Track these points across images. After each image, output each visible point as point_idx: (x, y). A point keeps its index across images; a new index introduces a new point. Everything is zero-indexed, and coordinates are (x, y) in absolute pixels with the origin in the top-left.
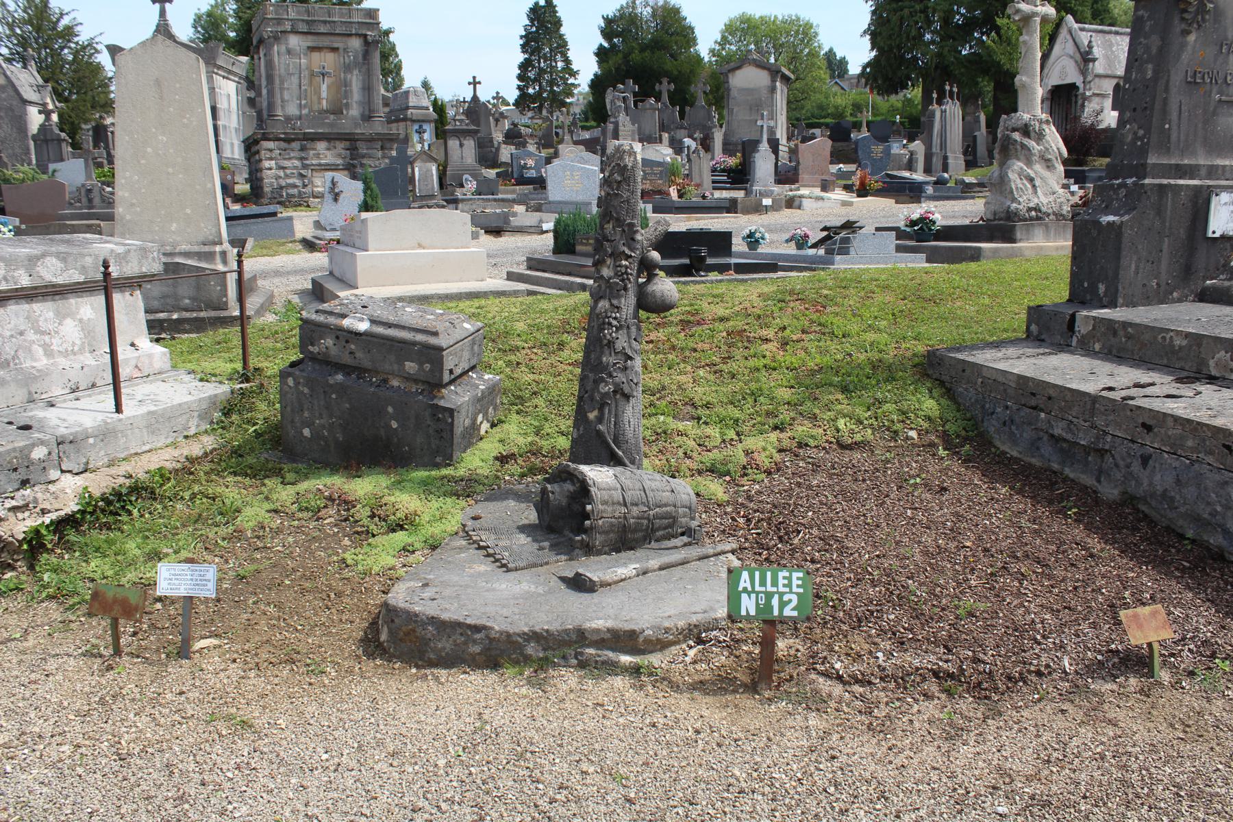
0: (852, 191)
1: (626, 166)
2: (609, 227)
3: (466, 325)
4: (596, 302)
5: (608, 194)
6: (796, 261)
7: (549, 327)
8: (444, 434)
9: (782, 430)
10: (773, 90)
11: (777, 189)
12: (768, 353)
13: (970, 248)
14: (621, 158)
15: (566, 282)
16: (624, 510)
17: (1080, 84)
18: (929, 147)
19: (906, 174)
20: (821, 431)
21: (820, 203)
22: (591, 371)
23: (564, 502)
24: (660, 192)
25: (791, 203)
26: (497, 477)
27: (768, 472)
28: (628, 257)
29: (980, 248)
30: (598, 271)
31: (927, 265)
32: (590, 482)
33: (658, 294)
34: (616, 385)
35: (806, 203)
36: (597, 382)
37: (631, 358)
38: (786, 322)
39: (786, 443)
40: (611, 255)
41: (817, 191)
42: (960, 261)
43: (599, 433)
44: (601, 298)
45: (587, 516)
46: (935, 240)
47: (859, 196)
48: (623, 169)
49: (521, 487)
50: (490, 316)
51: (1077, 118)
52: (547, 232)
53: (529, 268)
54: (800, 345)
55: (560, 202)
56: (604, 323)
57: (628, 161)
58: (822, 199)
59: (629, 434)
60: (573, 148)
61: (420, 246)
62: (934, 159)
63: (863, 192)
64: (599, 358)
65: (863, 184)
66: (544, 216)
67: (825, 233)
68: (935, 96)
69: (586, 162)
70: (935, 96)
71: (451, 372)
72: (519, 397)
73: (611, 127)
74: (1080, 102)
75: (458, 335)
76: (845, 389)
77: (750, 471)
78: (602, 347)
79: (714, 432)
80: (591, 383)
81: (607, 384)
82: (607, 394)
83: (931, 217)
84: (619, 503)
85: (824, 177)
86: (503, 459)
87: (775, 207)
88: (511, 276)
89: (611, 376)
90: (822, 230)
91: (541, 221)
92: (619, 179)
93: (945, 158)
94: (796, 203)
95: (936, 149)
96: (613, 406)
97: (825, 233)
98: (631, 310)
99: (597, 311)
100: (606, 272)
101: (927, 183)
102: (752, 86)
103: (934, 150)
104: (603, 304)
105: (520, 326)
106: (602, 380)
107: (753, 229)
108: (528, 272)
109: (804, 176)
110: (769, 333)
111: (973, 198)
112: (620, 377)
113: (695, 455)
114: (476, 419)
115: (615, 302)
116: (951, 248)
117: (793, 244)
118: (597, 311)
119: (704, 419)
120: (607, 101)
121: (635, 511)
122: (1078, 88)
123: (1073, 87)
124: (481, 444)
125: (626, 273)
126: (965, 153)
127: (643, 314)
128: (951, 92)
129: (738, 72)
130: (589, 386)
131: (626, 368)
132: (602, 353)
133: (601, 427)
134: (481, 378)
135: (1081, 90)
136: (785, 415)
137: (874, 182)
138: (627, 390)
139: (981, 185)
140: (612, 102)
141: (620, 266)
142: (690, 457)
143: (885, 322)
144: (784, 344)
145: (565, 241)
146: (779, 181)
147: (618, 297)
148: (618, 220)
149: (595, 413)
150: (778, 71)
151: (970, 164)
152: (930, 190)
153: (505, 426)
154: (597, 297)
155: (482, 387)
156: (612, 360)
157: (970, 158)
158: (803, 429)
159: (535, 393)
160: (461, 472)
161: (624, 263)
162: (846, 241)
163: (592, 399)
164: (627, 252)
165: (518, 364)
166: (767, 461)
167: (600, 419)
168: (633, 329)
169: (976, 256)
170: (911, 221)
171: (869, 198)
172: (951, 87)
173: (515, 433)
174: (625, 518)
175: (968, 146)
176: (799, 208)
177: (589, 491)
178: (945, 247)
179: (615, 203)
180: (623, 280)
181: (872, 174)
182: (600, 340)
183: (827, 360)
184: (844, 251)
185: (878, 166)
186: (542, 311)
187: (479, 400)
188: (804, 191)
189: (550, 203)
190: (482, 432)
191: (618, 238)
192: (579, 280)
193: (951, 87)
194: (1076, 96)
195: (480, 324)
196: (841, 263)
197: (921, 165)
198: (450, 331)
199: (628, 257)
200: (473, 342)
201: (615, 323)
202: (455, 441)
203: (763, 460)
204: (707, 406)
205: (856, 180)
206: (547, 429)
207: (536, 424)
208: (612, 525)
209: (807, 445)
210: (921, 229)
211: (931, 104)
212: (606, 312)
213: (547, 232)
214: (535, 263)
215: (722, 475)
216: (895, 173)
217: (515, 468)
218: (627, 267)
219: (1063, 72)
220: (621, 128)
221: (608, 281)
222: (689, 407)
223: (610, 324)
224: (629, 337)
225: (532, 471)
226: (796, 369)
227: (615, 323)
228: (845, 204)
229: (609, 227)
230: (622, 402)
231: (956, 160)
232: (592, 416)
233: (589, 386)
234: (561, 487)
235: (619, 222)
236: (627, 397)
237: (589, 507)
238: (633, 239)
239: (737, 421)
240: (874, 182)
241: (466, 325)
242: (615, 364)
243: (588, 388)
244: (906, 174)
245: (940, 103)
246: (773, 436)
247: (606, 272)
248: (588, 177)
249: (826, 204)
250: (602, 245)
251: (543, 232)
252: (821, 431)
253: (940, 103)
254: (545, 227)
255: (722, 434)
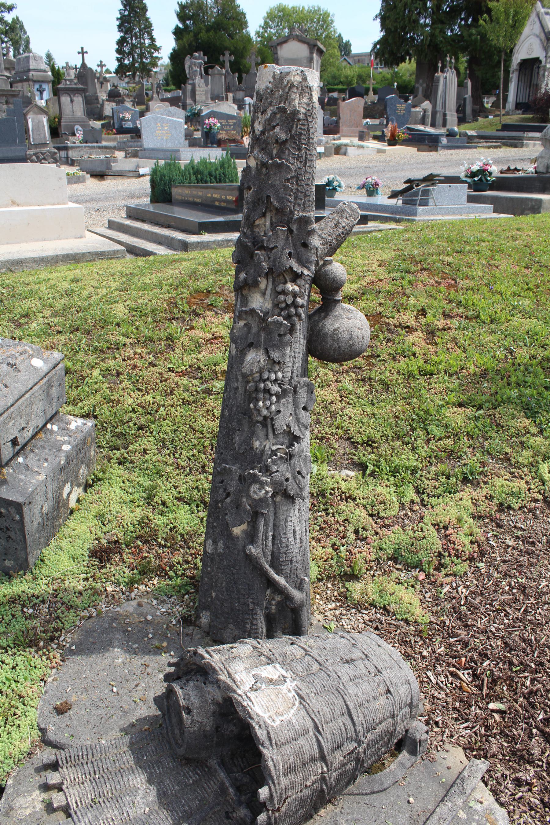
0: (384, 141)
1: (295, 113)
2: (264, 224)
3: (37, 363)
4: (241, 353)
5: (263, 165)
6: (376, 211)
7: (153, 311)
8: (12, 534)
9: (476, 484)
10: (311, 60)
11: (324, 138)
12: (416, 349)
13: (531, 200)
14: (286, 98)
15: (167, 237)
16: (320, 767)
17: (542, 58)
18: (434, 107)
19: (421, 127)
20: (523, 483)
21: (361, 151)
22: (236, 459)
23: (209, 724)
24: (234, 141)
25: (338, 150)
26: (96, 593)
27: (471, 559)
28: (296, 277)
29: (540, 201)
30: (245, 301)
31: (495, 215)
32: (261, 734)
33: (344, 336)
34: (276, 485)
35: (350, 150)
36: (247, 481)
37: (296, 439)
38: (424, 301)
39: (484, 507)
40: (270, 272)
41: (356, 140)
42: (522, 213)
43: (250, 558)
44: (251, 345)
45: (262, 807)
46: (491, 189)
47: (390, 145)
48: (290, 119)
49: (130, 607)
50: (85, 293)
51: (537, 87)
52: (143, 175)
53: (129, 217)
54: (448, 335)
55: (153, 150)
56: (257, 390)
57: (298, 103)
58: (362, 147)
59: (294, 550)
60: (161, 104)
61: (14, 203)
62: (438, 115)
63: (393, 141)
64: (248, 442)
65: (393, 135)
66: (141, 161)
67: (407, 185)
68: (440, 65)
69: (173, 116)
70: (440, 65)
71: (14, 442)
72: (121, 436)
73: (189, 87)
74: (541, 73)
75: (21, 382)
76: (530, 411)
77: (447, 560)
78: (253, 424)
79: (385, 490)
80: (236, 481)
81: (262, 485)
82: (263, 501)
83: (490, 169)
84: (314, 759)
85: (361, 129)
86: (101, 555)
87: (326, 154)
88: (112, 225)
89: (267, 470)
90: (405, 183)
91: (138, 166)
92: (283, 136)
93: (445, 115)
94: (343, 150)
95: (439, 108)
96: (272, 514)
97: (407, 185)
98: (298, 363)
99: (246, 369)
100: (258, 302)
101: (442, 135)
102: (295, 57)
103: (438, 109)
104: (254, 358)
105: (120, 310)
106: (255, 479)
107: (331, 177)
108: (128, 222)
109: (343, 128)
110: (408, 318)
111: (475, 147)
112: (282, 471)
113: (369, 534)
114: (60, 494)
115: (275, 355)
116: (512, 199)
117: (364, 191)
118: (246, 369)
119: (371, 467)
120: (186, 66)
121: (338, 758)
122: (540, 62)
123: (537, 60)
124: (71, 524)
125: (295, 305)
126: (458, 111)
127: (313, 361)
128: (450, 62)
129: (285, 46)
130: (233, 485)
131: (291, 456)
132: (253, 434)
133: (253, 550)
134: (65, 430)
135: (543, 63)
136: (472, 459)
137: (402, 134)
138: (292, 489)
139: (480, 137)
140: (190, 67)
141: (284, 292)
142: (364, 539)
143: (527, 302)
144: (431, 334)
145: (161, 191)
146: (325, 133)
147: (281, 345)
148: (279, 211)
149: (244, 527)
150: (315, 45)
151: (461, 121)
152: (444, 140)
153: (104, 488)
154: (242, 343)
155: (66, 448)
156: (270, 445)
157: (461, 115)
158: (501, 483)
159: (141, 428)
160: (42, 587)
161: (290, 287)
162: (426, 193)
163: (238, 506)
164: (297, 268)
165: (119, 374)
166: (466, 541)
167: (252, 536)
168: (303, 392)
169: (535, 208)
170: (472, 172)
171: (398, 147)
172: (451, 58)
173: (117, 503)
174: (323, 779)
175: (459, 106)
176: (345, 154)
177: (259, 755)
178: (506, 198)
179: (276, 180)
180: (288, 317)
181: (399, 127)
182: (248, 413)
183: (486, 361)
184: (424, 203)
185: (402, 121)
186: (145, 288)
187: (62, 469)
188: (344, 141)
189: (145, 150)
190: (73, 503)
191: (280, 243)
192: (179, 236)
193: (451, 58)
194: (539, 68)
195: (57, 355)
196: (423, 215)
197: (429, 121)
198: (8, 380)
199: (296, 277)
200: (50, 385)
201: (275, 389)
202: (29, 540)
203: (462, 540)
204: (369, 443)
205: (388, 132)
206: (163, 495)
207: (148, 484)
208: (302, 800)
209: (509, 507)
210: (480, 180)
211: (436, 71)
212: (261, 372)
213: (143, 175)
214: (134, 214)
215: (409, 567)
216: (412, 126)
217: (119, 570)
218: (295, 295)
219: (530, 49)
220: (197, 88)
221: (263, 320)
222: (343, 443)
223: (267, 391)
224: (296, 406)
225: (146, 572)
226: (456, 373)
227: (275, 389)
228: (380, 151)
229: (264, 224)
230: (284, 507)
231: (452, 117)
232: (237, 531)
233: (233, 485)
234: (201, 695)
235: (283, 216)
236: (291, 499)
237: (263, 792)
238: (305, 245)
239: (414, 472)
240: (402, 134)
241: (37, 363)
242: (274, 453)
243: (231, 489)
244: (421, 127)
245: (442, 71)
246: (467, 494)
247: (258, 302)
248: (175, 128)
249: (365, 151)
250: (252, 256)
251: (140, 176)
252: (524, 486)
253: (442, 71)
254: (142, 171)
255: (400, 495)
